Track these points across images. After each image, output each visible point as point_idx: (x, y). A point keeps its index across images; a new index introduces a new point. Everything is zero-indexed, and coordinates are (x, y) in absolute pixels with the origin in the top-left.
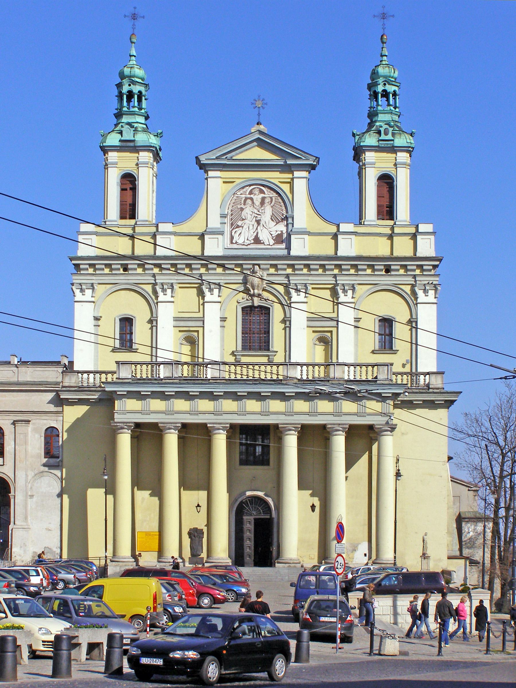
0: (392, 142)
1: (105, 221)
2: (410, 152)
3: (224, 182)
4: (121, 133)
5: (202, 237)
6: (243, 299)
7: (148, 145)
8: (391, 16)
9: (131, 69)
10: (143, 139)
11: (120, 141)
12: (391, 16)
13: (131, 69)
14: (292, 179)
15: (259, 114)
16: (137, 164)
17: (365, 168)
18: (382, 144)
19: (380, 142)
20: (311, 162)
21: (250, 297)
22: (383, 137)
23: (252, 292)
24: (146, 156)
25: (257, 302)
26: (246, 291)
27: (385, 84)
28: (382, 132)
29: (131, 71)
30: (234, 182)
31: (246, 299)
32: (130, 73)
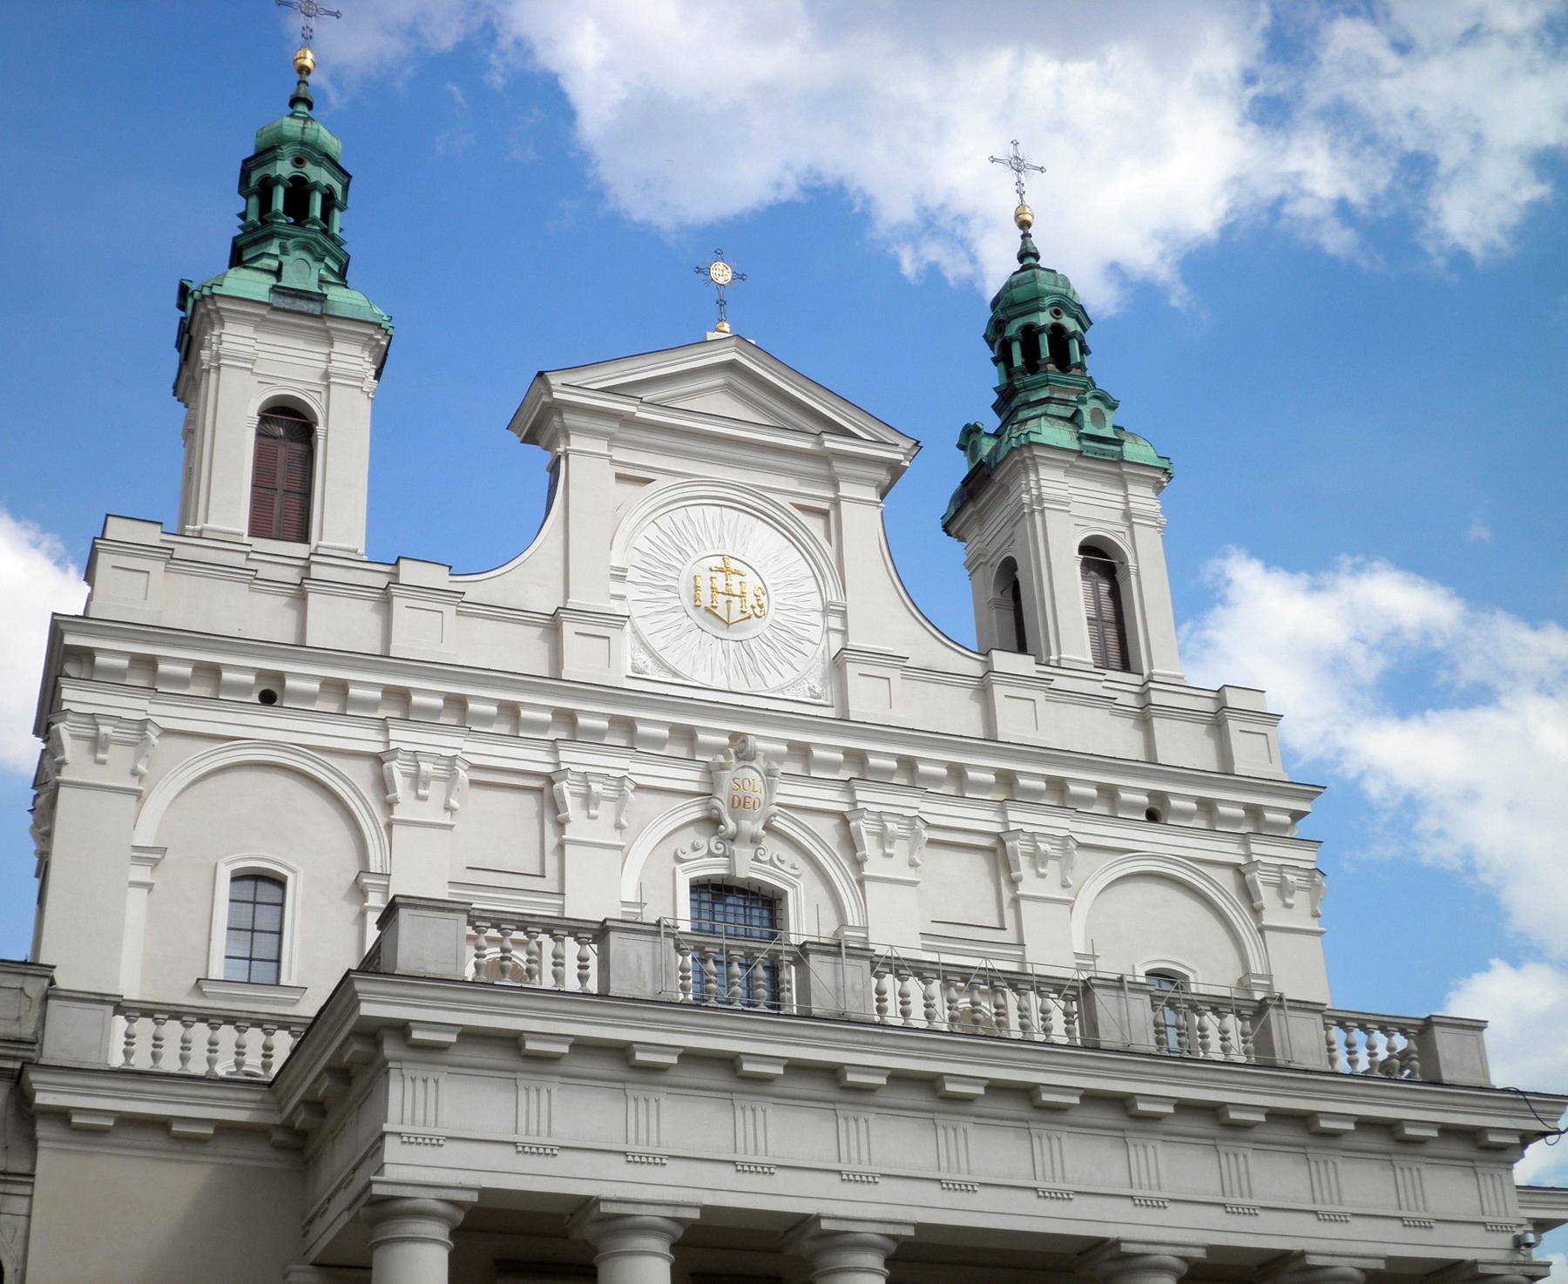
0: (1117, 449)
1: (198, 527)
2: (1159, 488)
3: (619, 477)
4: (278, 273)
5: (553, 626)
6: (695, 849)
7: (371, 320)
8: (1036, 168)
9: (305, 123)
10: (354, 302)
11: (274, 290)
12: (1036, 168)
13: (305, 123)
14: (836, 503)
15: (721, 303)
16: (326, 375)
17: (1042, 512)
18: (1089, 449)
19: (1085, 443)
20: (901, 457)
21: (720, 846)
22: (1088, 428)
23: (730, 826)
24: (354, 359)
25: (746, 868)
26: (712, 822)
27: (1057, 312)
28: (1087, 417)
29: (304, 128)
30: (650, 481)
31: (705, 851)
32: (303, 132)
